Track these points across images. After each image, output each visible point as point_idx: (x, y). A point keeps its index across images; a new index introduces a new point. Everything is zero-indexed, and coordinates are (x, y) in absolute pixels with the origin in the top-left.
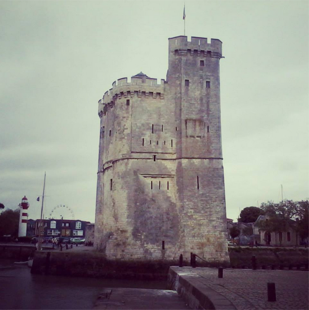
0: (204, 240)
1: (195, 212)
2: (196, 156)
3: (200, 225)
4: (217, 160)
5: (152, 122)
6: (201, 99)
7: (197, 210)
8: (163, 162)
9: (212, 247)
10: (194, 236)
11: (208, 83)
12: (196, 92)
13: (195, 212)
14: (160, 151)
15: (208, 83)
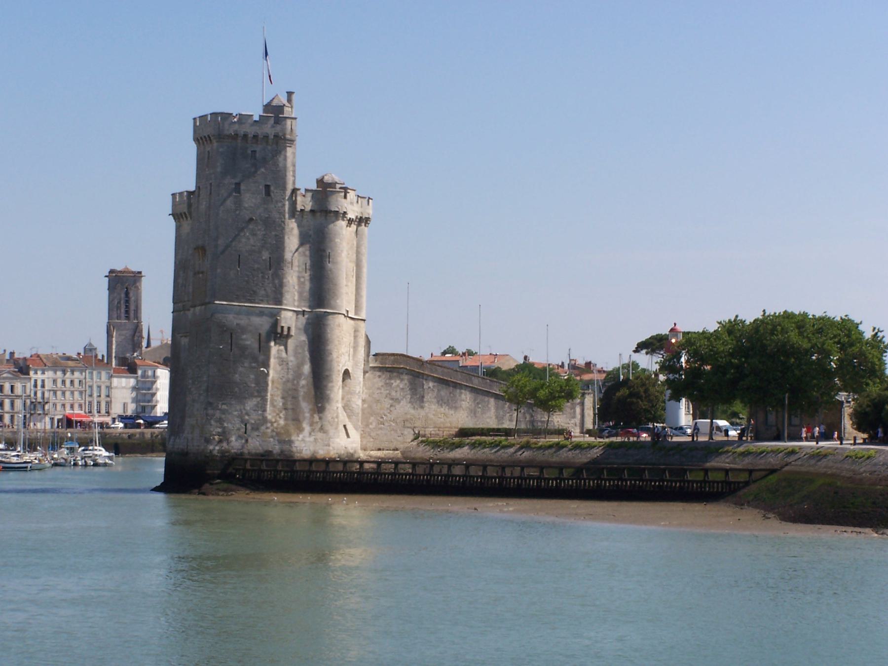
3: (194, 401)
14: (186, 299)
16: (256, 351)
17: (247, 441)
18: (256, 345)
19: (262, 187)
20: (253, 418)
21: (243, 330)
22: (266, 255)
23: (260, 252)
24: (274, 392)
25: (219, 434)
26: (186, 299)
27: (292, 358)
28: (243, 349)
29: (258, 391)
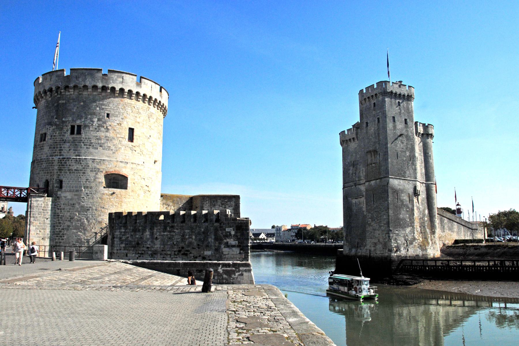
0: (376, 241)
1: (372, 221)
2: (373, 179)
3: (374, 230)
4: (385, 179)
5: (353, 159)
6: (375, 134)
7: (373, 219)
8: (359, 186)
9: (381, 246)
10: (371, 238)
11: (378, 119)
12: (372, 129)
13: (372, 221)
14: (357, 179)
15: (378, 119)
16: (408, 203)
17: (408, 250)
18: (408, 199)
19: (403, 120)
20: (410, 238)
21: (402, 191)
22: (408, 154)
23: (405, 152)
24: (417, 224)
25: (395, 247)
26: (357, 179)
27: (421, 207)
28: (402, 201)
29: (411, 224)
